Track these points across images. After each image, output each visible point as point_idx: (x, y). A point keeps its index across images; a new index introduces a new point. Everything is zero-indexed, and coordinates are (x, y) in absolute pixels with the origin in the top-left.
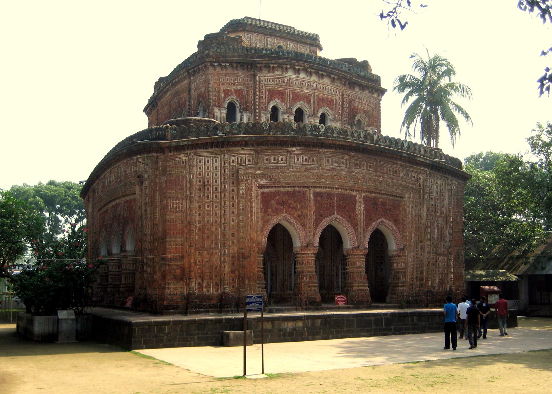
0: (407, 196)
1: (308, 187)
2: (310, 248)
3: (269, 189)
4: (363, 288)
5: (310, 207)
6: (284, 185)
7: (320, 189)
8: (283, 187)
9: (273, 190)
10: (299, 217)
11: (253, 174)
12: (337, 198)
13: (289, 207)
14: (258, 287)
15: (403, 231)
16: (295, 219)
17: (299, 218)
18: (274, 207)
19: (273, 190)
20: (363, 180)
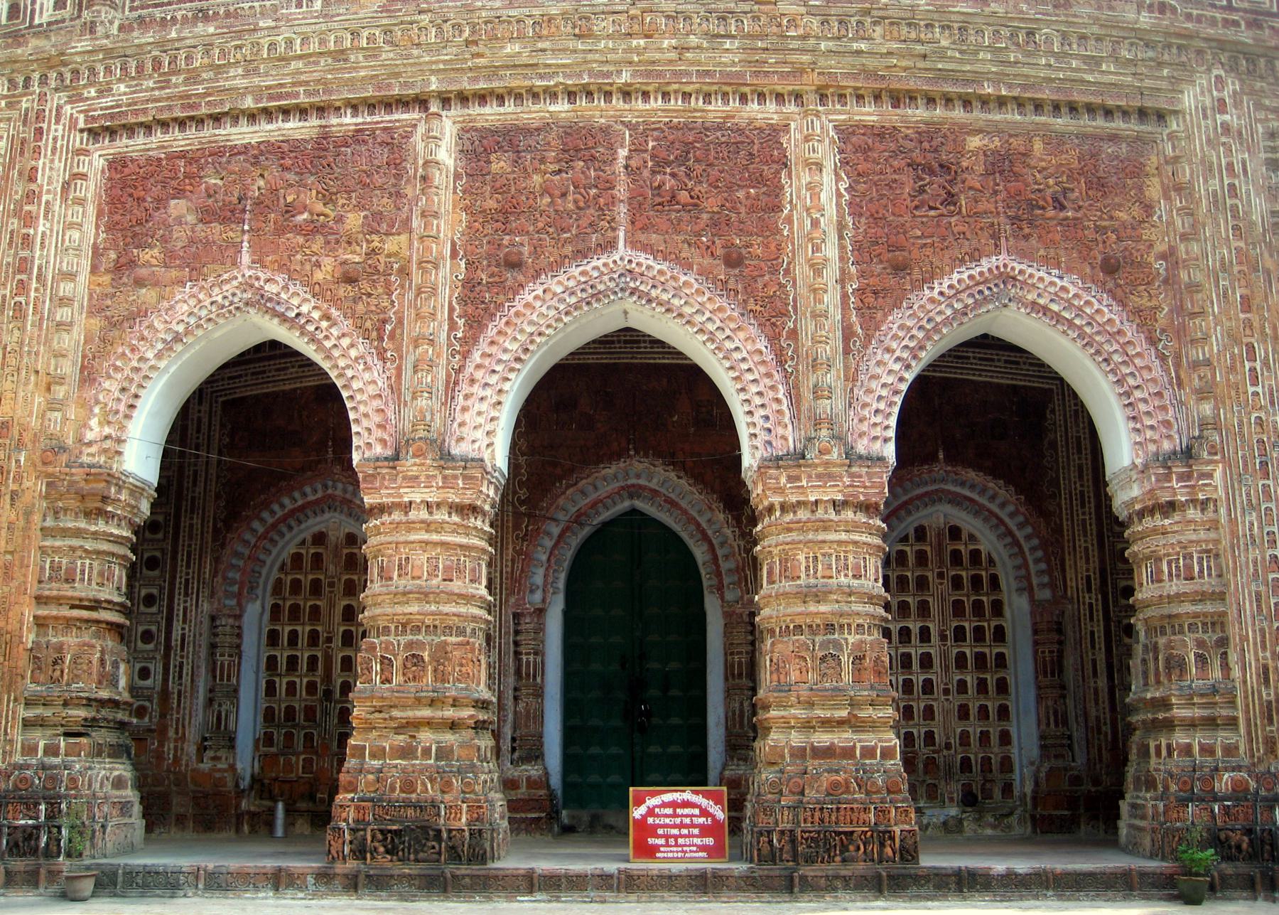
0: (1189, 99)
1: (421, 102)
2: (409, 464)
3: (158, 137)
4: (842, 738)
5: (423, 214)
6: (249, 103)
7: (510, 107)
8: (252, 117)
9: (179, 140)
10: (350, 280)
11: (48, 63)
12: (636, 150)
13: (280, 231)
14: (27, 724)
15: (1180, 333)
16: (318, 292)
17: (343, 290)
18: (180, 236)
19: (179, 140)
20: (815, 22)
